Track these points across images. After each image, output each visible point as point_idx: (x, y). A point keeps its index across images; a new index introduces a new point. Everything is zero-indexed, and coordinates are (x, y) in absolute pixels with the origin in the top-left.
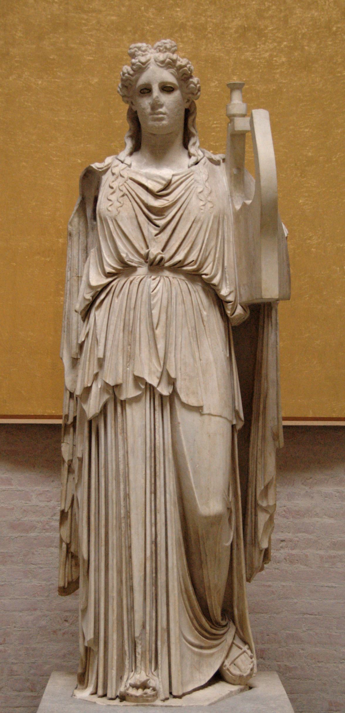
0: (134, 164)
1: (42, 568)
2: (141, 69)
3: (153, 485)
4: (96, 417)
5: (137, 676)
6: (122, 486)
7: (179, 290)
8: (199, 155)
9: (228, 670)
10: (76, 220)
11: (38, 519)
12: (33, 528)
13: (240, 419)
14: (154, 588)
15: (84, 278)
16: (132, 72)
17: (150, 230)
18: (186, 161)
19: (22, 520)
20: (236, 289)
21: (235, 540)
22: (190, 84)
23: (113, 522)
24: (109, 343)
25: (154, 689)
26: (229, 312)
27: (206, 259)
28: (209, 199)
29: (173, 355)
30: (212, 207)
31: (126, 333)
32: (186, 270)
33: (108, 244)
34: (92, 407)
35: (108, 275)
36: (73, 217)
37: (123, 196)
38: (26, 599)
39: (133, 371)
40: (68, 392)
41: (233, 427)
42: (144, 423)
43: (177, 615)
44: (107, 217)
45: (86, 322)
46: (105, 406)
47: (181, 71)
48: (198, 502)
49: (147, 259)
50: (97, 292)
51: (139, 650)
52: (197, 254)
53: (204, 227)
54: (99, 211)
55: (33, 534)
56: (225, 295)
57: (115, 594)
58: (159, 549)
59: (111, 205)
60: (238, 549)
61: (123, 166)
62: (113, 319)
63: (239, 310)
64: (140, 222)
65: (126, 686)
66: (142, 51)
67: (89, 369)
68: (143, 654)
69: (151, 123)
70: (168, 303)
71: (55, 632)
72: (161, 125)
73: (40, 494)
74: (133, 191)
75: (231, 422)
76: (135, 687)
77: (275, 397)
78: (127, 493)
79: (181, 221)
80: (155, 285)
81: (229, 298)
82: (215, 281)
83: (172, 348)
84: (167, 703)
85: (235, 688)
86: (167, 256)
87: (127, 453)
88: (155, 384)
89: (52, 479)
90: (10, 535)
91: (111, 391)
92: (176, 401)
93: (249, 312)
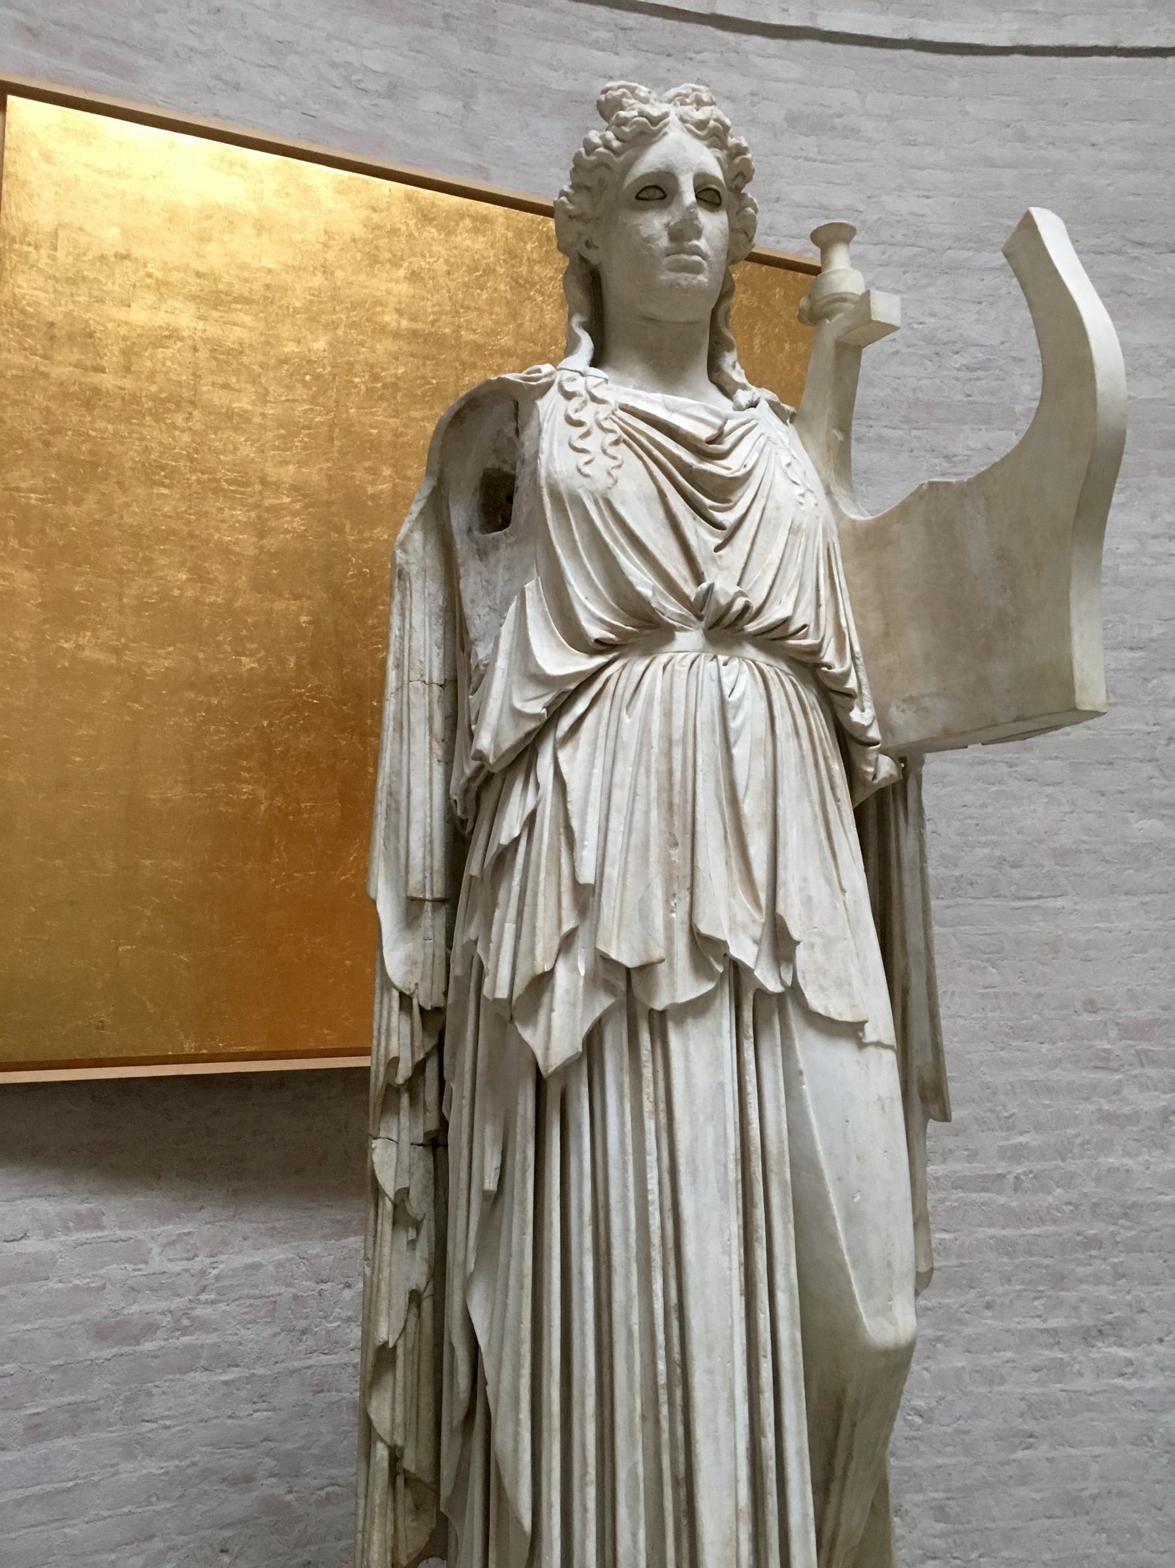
1: (167, 1427)
2: (648, 132)
10: (418, 536)
11: (163, 1305)
12: (151, 1329)
16: (616, 144)
17: (701, 537)
19: (125, 1312)
22: (746, 206)
32: (797, 649)
34: (557, 1034)
35: (602, 646)
36: (411, 530)
37: (616, 443)
38: (130, 1513)
40: (396, 994)
44: (581, 492)
47: (738, 160)
50: (564, 693)
54: (549, 476)
55: (147, 1346)
59: (587, 463)
62: (624, 771)
66: (637, 97)
69: (666, 277)
72: (695, 282)
73: (173, 1243)
89: (198, 1204)
90: (93, 1354)
91: (622, 986)
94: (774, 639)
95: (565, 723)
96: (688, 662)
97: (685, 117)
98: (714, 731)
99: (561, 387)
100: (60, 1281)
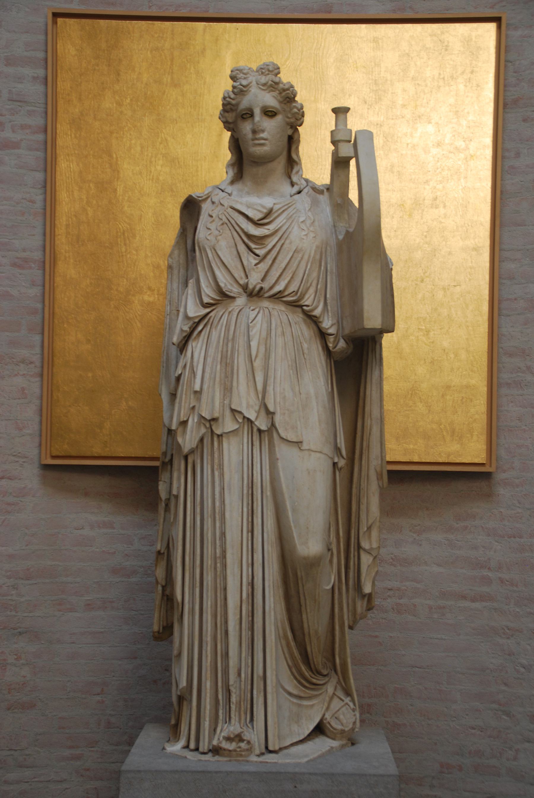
0: (235, 193)
3: (250, 524)
4: (192, 451)
5: (232, 728)
6: (218, 524)
7: (279, 321)
8: (302, 184)
9: (329, 723)
13: (343, 457)
14: (250, 633)
15: (182, 310)
16: (232, 96)
17: (250, 260)
18: (288, 189)
20: (338, 322)
21: (337, 583)
22: (293, 109)
23: (208, 562)
24: (207, 376)
25: (249, 742)
26: (330, 345)
27: (308, 289)
28: (311, 229)
29: (272, 387)
30: (314, 237)
31: (224, 365)
33: (206, 274)
39: (230, 405)
40: (166, 429)
41: (335, 464)
42: (241, 458)
43: (274, 662)
45: (183, 354)
46: (202, 440)
47: (284, 94)
48: (297, 542)
49: (246, 289)
50: (195, 323)
51: (234, 699)
52: (298, 285)
53: (306, 257)
54: (198, 239)
56: (327, 327)
57: (209, 639)
58: (255, 591)
59: (210, 234)
60: (340, 593)
61: (224, 194)
62: (211, 351)
63: (342, 344)
64: (240, 251)
65: (219, 739)
66: (244, 74)
67: (185, 402)
68: (239, 703)
70: (267, 334)
71: (155, 682)
74: (233, 219)
75: (332, 459)
76: (228, 739)
77: (378, 434)
78: (223, 531)
79: (282, 251)
80: (254, 316)
81: (331, 331)
82: (317, 312)
83: (271, 381)
84: (261, 759)
85: (335, 744)
86: (266, 285)
87: (223, 489)
88: (253, 418)
91: (208, 425)
92: (275, 435)
93: (352, 346)
94: (277, 297)
95: (196, 333)
96: (238, 310)
98: (244, 336)
99: (211, 200)
100: (97, 548)
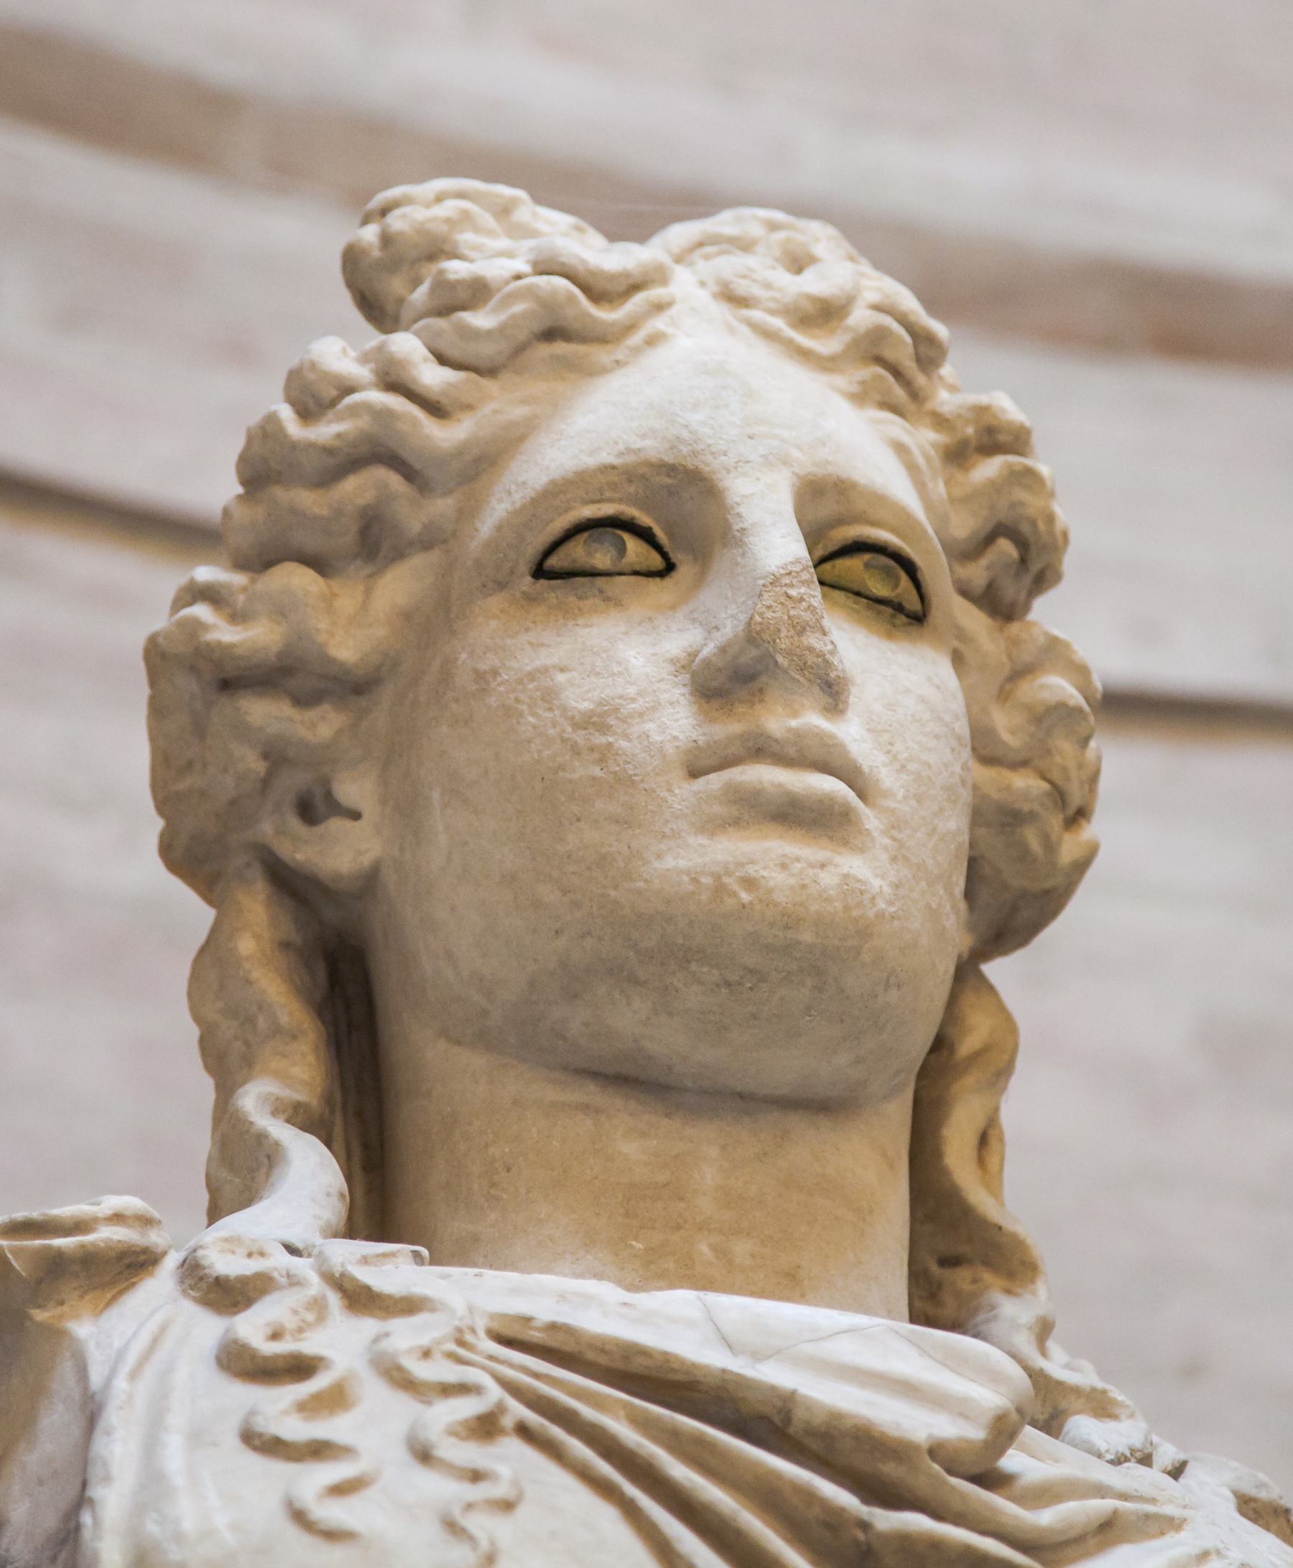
16: (432, 376)
97: (742, 287)
